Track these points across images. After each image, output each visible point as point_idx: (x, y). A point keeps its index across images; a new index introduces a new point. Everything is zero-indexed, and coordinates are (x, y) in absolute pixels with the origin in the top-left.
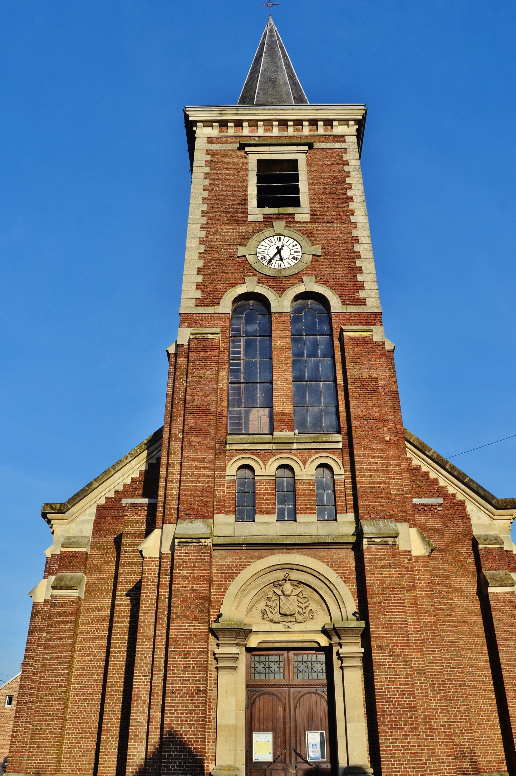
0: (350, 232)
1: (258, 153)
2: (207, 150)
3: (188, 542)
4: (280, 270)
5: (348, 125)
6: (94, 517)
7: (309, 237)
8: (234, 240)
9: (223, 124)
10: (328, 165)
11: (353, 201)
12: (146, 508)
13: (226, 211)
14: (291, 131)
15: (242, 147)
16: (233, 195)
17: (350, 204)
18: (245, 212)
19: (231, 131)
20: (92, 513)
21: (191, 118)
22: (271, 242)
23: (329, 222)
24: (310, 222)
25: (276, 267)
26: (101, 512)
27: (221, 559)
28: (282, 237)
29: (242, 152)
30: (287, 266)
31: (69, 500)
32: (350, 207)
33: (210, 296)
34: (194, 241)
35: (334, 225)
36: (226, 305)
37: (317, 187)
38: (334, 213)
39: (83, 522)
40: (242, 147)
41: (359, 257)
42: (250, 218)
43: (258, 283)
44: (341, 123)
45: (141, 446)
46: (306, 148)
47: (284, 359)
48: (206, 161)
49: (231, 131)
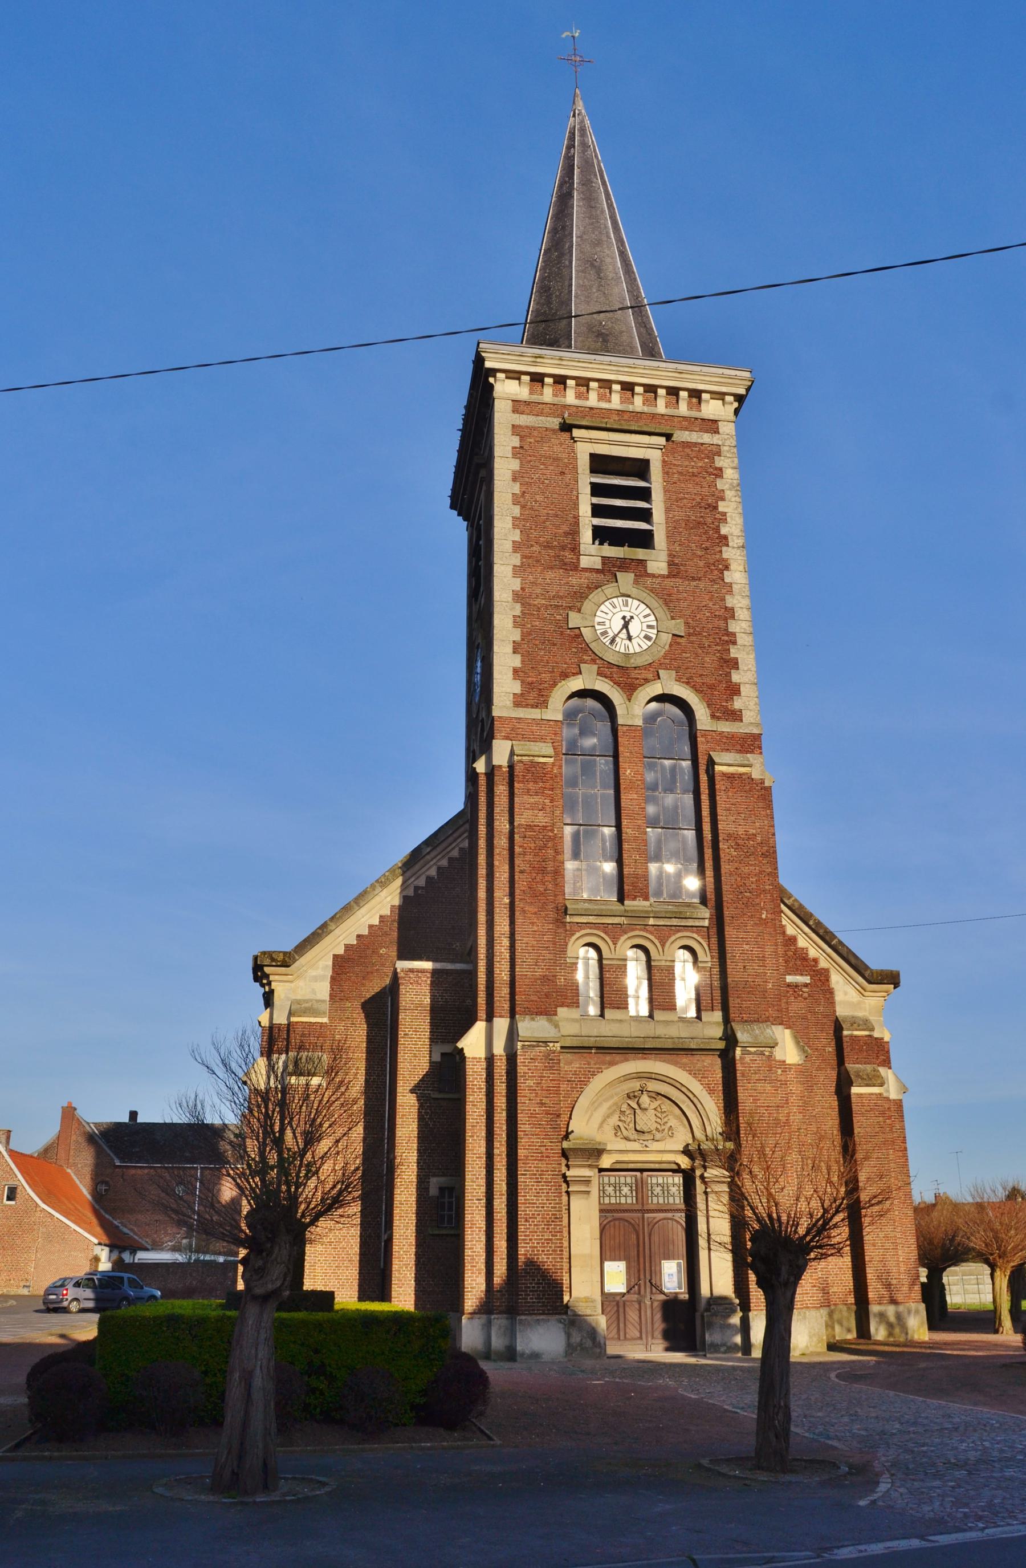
0: (723, 600)
1: (591, 441)
2: (513, 426)
3: (534, 1046)
4: (627, 656)
5: (723, 400)
6: (329, 973)
7: (666, 604)
8: (561, 597)
9: (537, 379)
10: (694, 475)
11: (728, 545)
12: (429, 975)
13: (548, 546)
14: (638, 403)
15: (566, 428)
16: (557, 516)
17: (724, 549)
18: (575, 549)
19: (548, 394)
20: (327, 966)
21: (488, 364)
22: (615, 607)
23: (694, 579)
24: (668, 577)
25: (622, 650)
26: (339, 962)
27: (572, 1064)
28: (630, 600)
29: (566, 435)
30: (638, 650)
31: (296, 947)
32: (725, 556)
33: (534, 693)
34: (505, 595)
35: (702, 584)
36: (555, 709)
37: (679, 515)
38: (701, 564)
39: (315, 979)
40: (566, 428)
41: (735, 643)
42: (585, 562)
43: (598, 674)
44: (714, 396)
45: (394, 871)
46: (662, 440)
47: (635, 796)
48: (514, 448)
49: (548, 394)
